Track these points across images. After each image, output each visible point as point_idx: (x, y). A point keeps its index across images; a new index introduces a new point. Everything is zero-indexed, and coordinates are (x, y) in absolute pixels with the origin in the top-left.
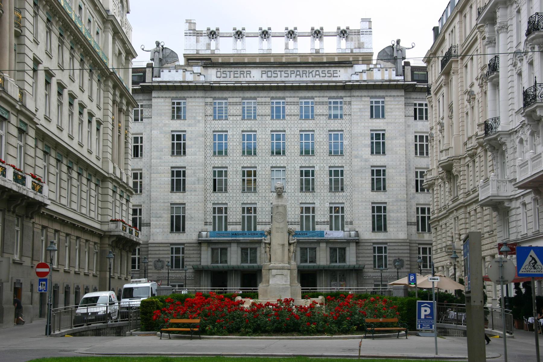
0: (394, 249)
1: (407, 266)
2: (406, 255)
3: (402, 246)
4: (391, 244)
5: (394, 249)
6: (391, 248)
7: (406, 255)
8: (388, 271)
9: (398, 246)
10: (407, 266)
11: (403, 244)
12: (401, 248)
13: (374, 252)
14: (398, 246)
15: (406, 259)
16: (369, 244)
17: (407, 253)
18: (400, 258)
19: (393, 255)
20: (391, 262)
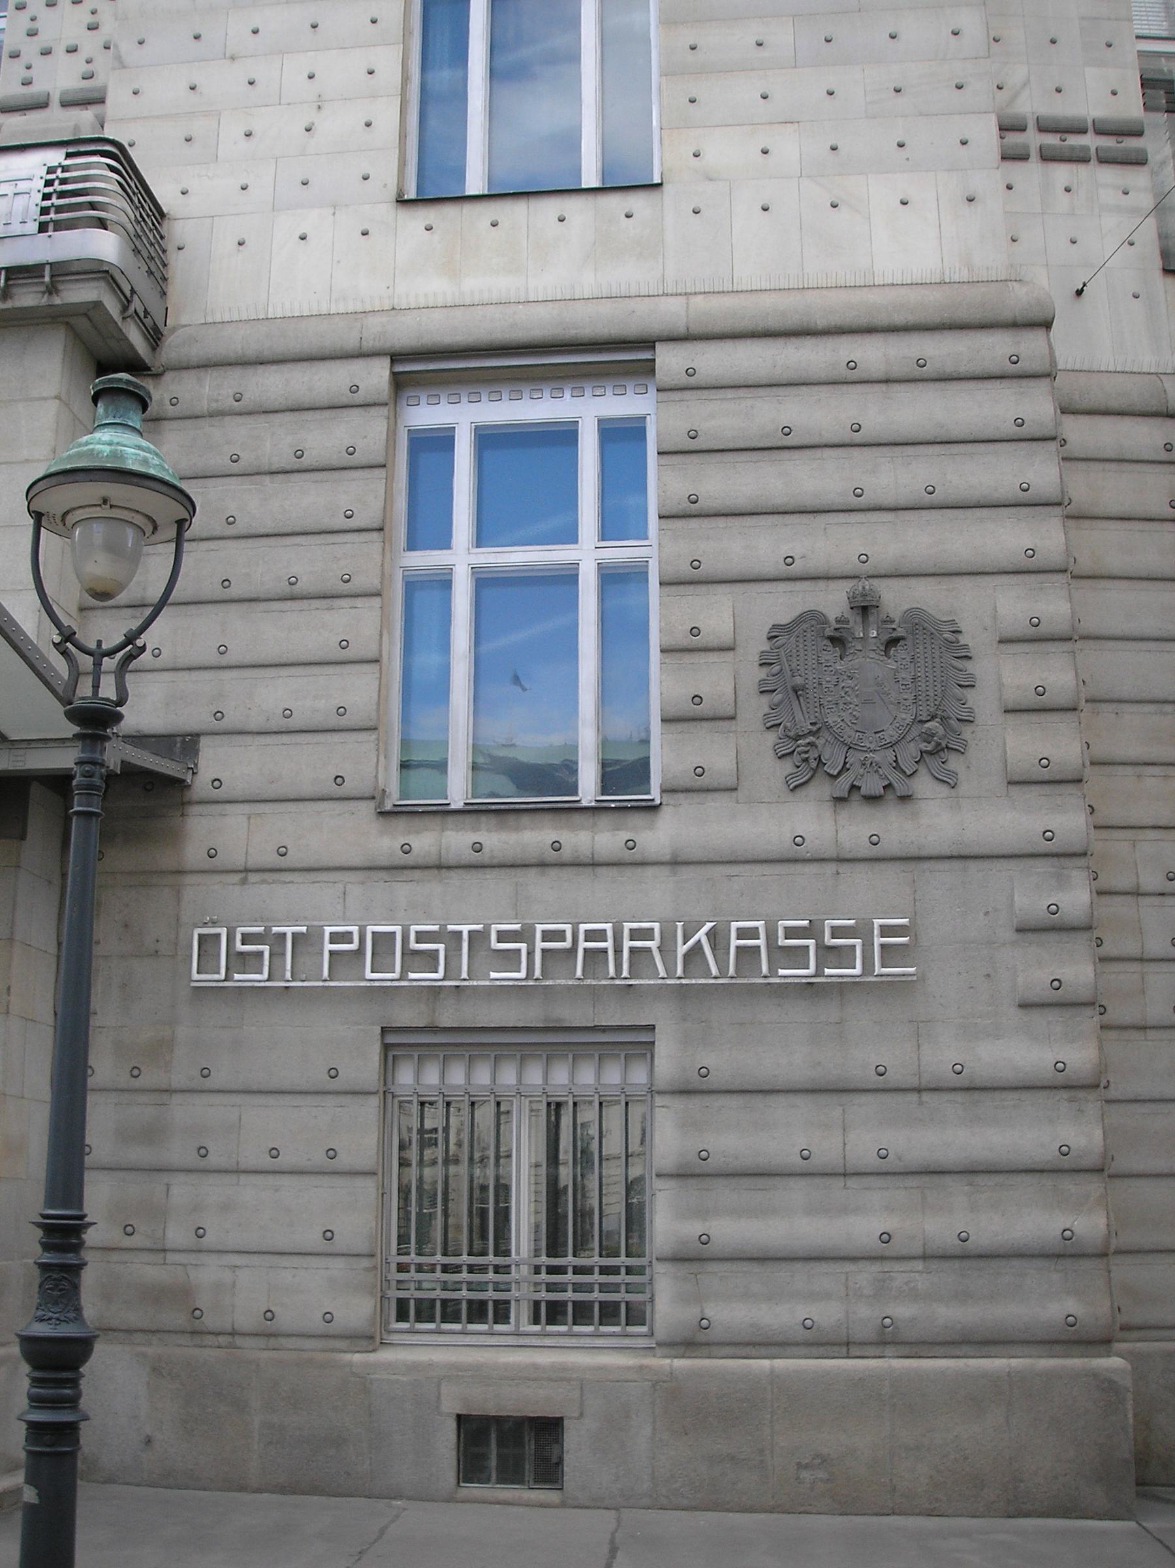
0: (783, 446)
1: (1028, 745)
2: (1008, 537)
3: (921, 377)
4: (713, 361)
5: (783, 446)
6: (722, 419)
7: (1008, 537)
8: (659, 836)
9: (851, 379)
10: (1028, 745)
11: (942, 351)
12: (914, 410)
13: (429, 527)
14: (851, 379)
15: (1014, 604)
16: (331, 380)
17: (1027, 503)
18: (896, 599)
19: (764, 546)
20: (716, 681)
